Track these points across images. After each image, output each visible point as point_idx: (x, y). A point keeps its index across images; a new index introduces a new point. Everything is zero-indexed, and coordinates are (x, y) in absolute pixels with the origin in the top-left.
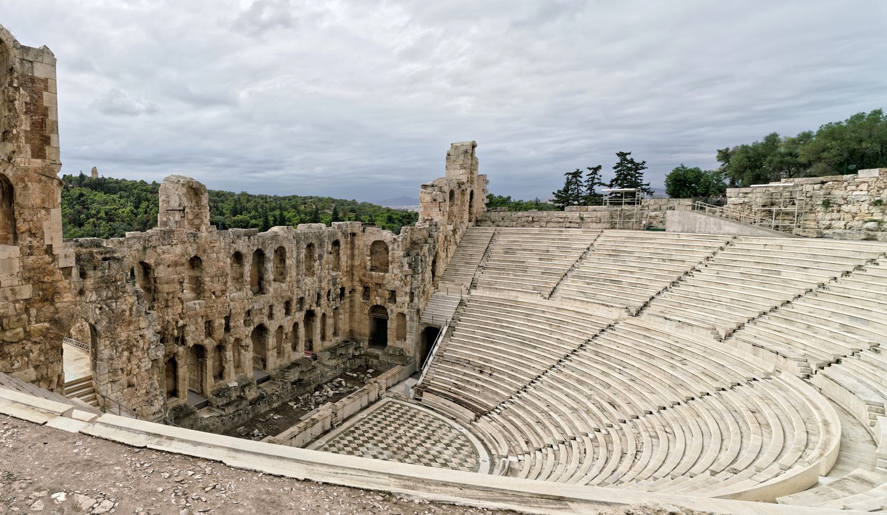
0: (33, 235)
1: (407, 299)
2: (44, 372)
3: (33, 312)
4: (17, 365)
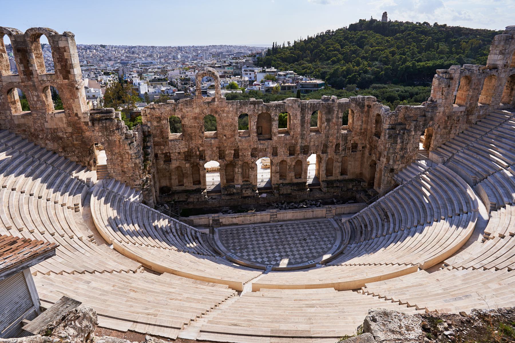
0: (68, 109)
1: (385, 160)
2: (81, 159)
3: (74, 137)
4: (70, 155)
